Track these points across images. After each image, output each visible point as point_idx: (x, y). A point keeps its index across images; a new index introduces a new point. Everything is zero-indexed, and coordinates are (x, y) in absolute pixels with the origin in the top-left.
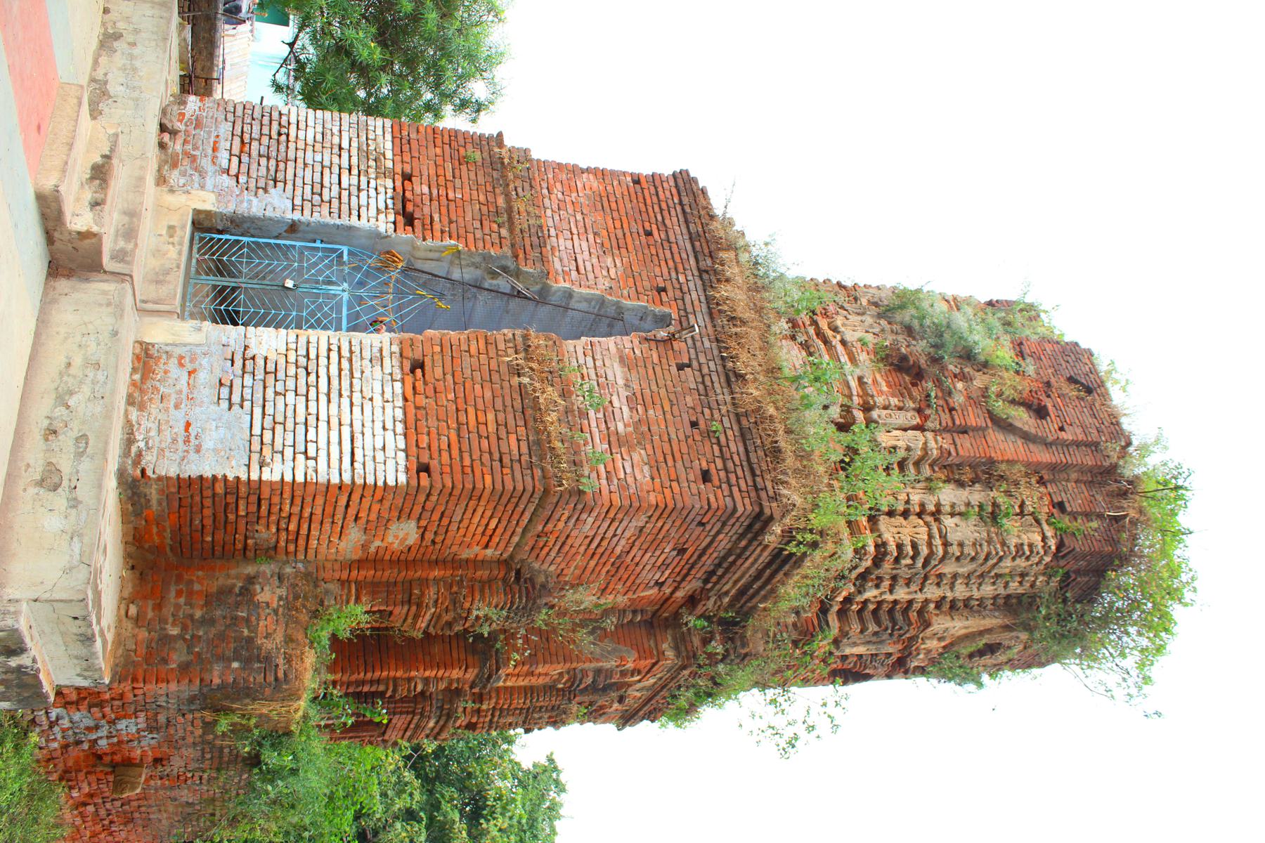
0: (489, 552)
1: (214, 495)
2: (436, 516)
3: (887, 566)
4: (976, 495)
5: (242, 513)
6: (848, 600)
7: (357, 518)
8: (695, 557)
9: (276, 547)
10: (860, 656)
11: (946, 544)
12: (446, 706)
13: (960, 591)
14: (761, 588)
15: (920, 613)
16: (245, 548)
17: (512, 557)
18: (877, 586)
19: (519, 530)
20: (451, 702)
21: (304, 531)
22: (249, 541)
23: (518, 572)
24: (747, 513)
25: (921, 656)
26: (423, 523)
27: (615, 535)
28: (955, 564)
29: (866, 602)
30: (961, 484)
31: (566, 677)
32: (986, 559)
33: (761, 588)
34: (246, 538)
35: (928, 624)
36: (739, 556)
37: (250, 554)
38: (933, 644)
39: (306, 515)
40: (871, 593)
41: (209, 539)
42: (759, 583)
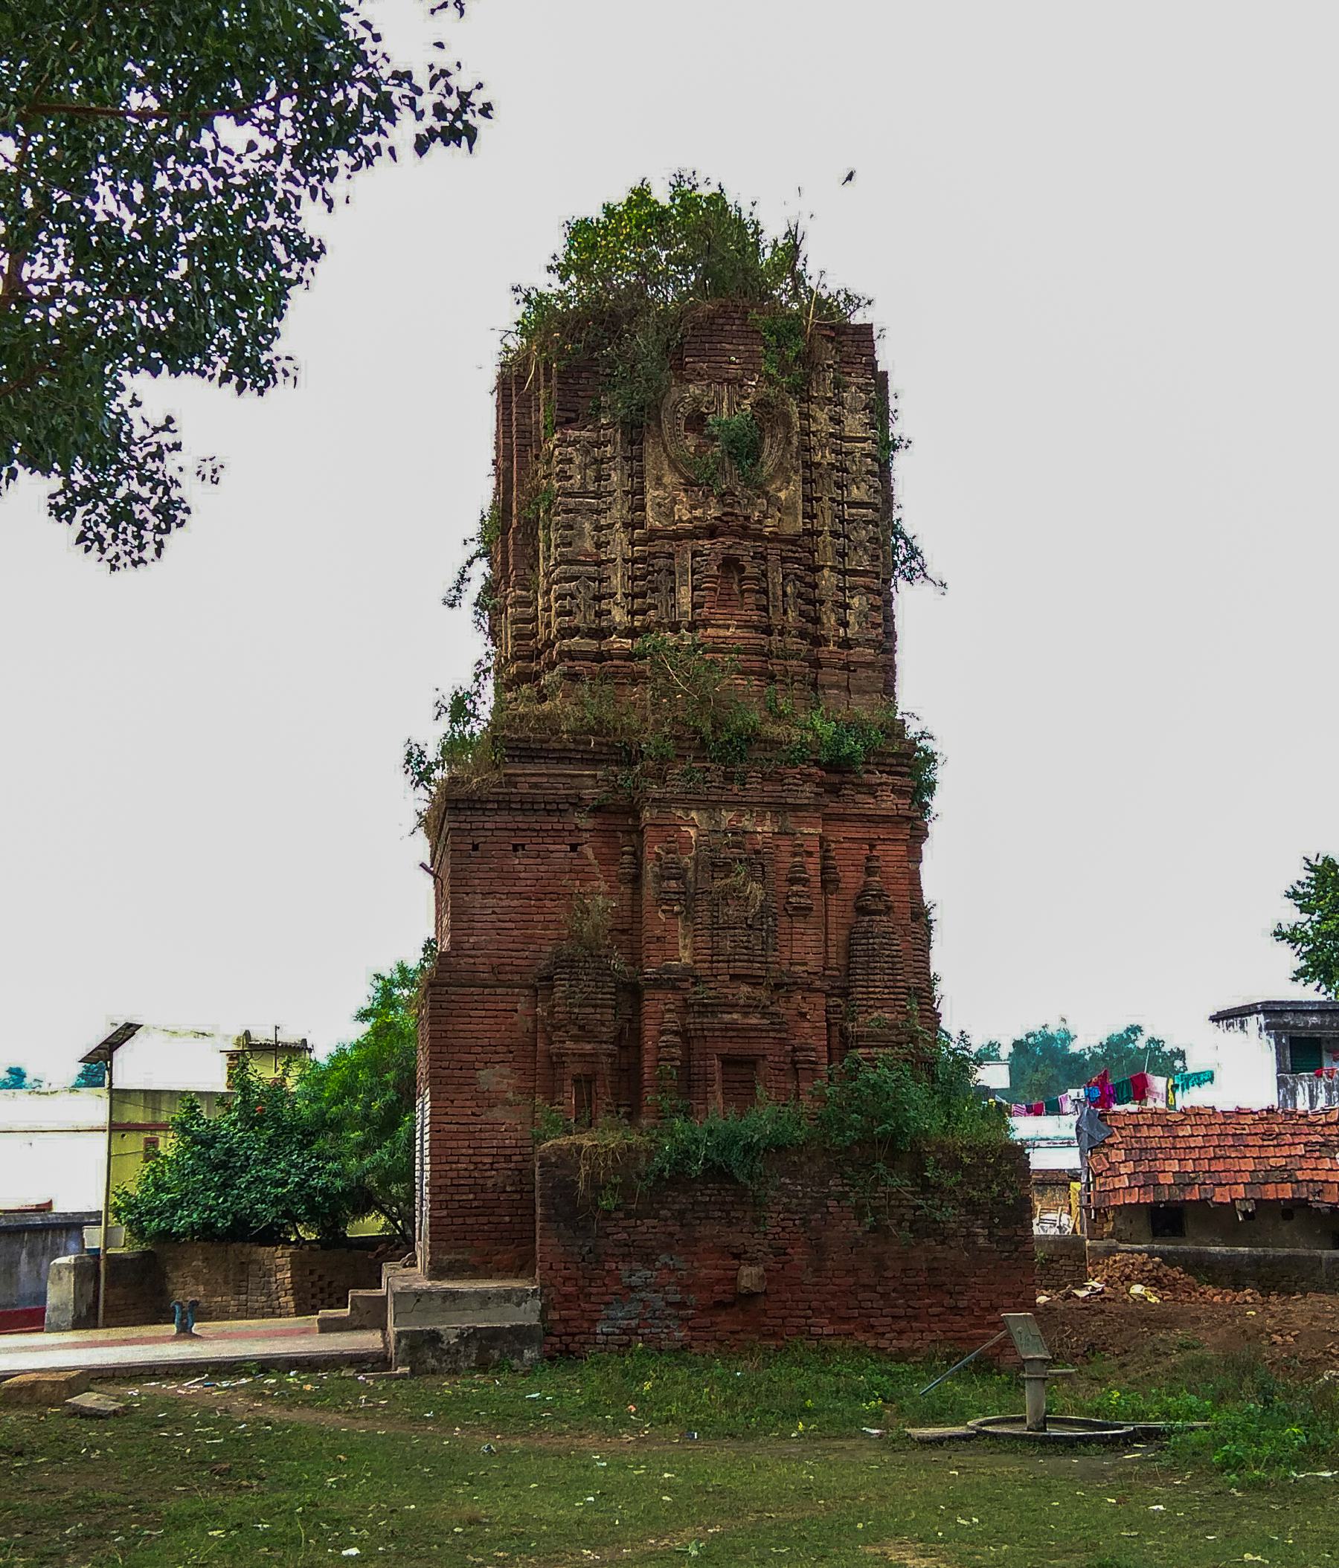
0: (519, 1007)
1: (448, 1216)
2: (472, 1057)
3: (577, 621)
4: (541, 533)
5: (471, 1196)
6: (632, 633)
7: (473, 1114)
8: (528, 833)
9: (520, 1170)
10: (694, 589)
11: (557, 565)
12: (696, 1008)
13: (617, 513)
14: (578, 751)
15: (643, 542)
16: (521, 1191)
17: (531, 987)
18: (609, 612)
19: (486, 991)
20: (692, 1005)
21: (494, 1151)
22: (508, 1189)
23: (541, 980)
24: (452, 818)
25: (698, 513)
26: (477, 1065)
27: (494, 913)
28: (578, 542)
29: (632, 613)
30: (536, 552)
31: (664, 907)
32: (570, 511)
33: (578, 751)
34: (505, 1192)
35: (653, 530)
36: (510, 802)
37: (527, 1188)
38: (682, 512)
39: (471, 1151)
40: (619, 616)
41: (507, 1219)
42: (572, 755)
